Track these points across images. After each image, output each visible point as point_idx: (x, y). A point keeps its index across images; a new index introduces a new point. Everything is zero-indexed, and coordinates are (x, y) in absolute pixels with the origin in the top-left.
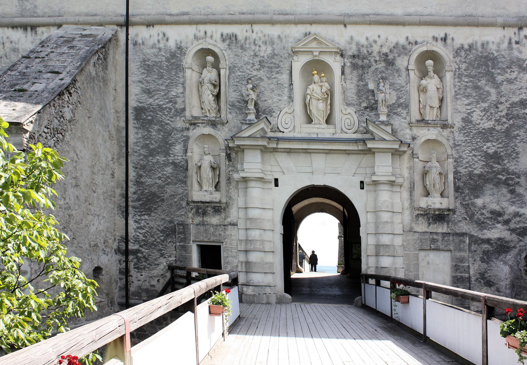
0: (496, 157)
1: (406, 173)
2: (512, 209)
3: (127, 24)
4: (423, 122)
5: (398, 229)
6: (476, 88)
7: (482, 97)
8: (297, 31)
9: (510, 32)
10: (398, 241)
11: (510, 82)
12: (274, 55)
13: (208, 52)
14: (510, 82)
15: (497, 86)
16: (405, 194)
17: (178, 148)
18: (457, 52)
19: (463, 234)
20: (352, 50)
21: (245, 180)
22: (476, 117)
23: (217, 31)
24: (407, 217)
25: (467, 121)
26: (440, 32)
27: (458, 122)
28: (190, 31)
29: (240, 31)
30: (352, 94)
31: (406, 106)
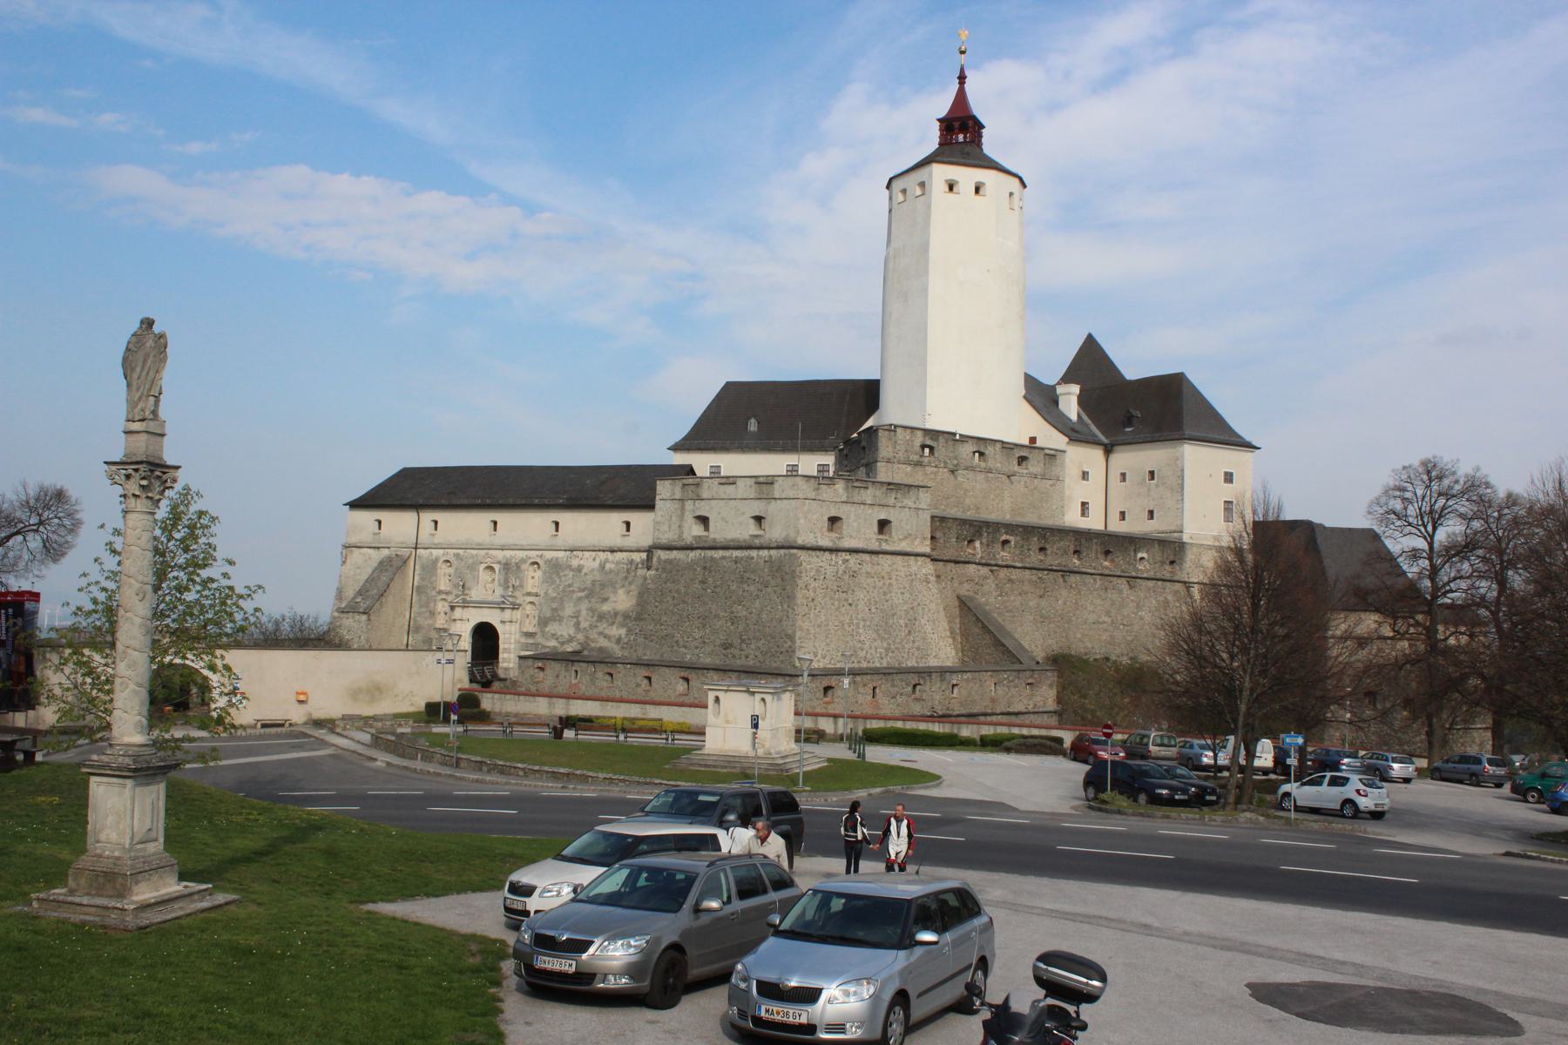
0: (555, 610)
1: (519, 617)
2: (559, 633)
3: (416, 548)
4: (529, 594)
5: (513, 641)
6: (551, 578)
7: (553, 582)
8: (483, 553)
9: (568, 553)
10: (512, 646)
11: (565, 576)
12: (473, 563)
13: (448, 561)
14: (565, 576)
15: (560, 578)
16: (518, 625)
17: (432, 605)
18: (545, 562)
19: (539, 644)
20: (504, 562)
21: (455, 620)
22: (550, 592)
23: (452, 552)
24: (518, 636)
25: (546, 593)
26: (540, 553)
27: (542, 594)
28: (441, 551)
29: (460, 551)
30: (502, 581)
31: (522, 586)
